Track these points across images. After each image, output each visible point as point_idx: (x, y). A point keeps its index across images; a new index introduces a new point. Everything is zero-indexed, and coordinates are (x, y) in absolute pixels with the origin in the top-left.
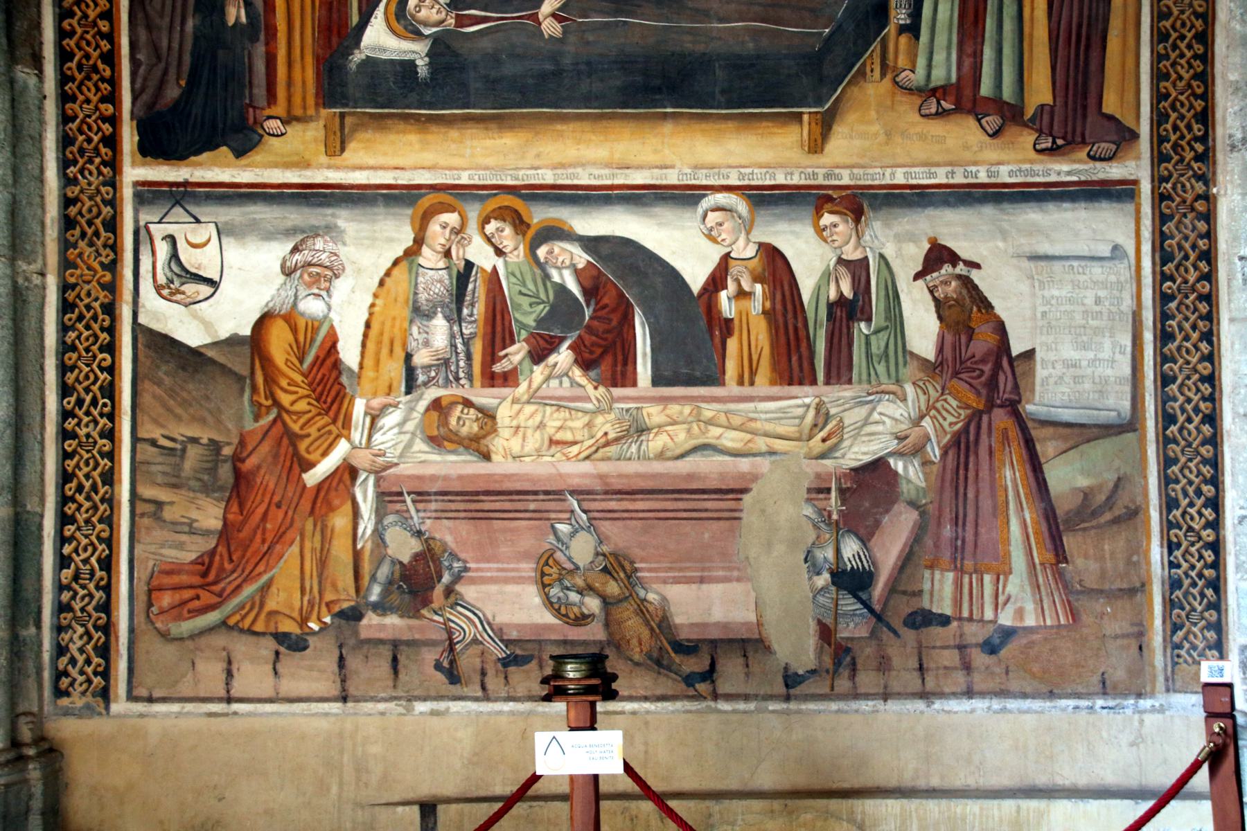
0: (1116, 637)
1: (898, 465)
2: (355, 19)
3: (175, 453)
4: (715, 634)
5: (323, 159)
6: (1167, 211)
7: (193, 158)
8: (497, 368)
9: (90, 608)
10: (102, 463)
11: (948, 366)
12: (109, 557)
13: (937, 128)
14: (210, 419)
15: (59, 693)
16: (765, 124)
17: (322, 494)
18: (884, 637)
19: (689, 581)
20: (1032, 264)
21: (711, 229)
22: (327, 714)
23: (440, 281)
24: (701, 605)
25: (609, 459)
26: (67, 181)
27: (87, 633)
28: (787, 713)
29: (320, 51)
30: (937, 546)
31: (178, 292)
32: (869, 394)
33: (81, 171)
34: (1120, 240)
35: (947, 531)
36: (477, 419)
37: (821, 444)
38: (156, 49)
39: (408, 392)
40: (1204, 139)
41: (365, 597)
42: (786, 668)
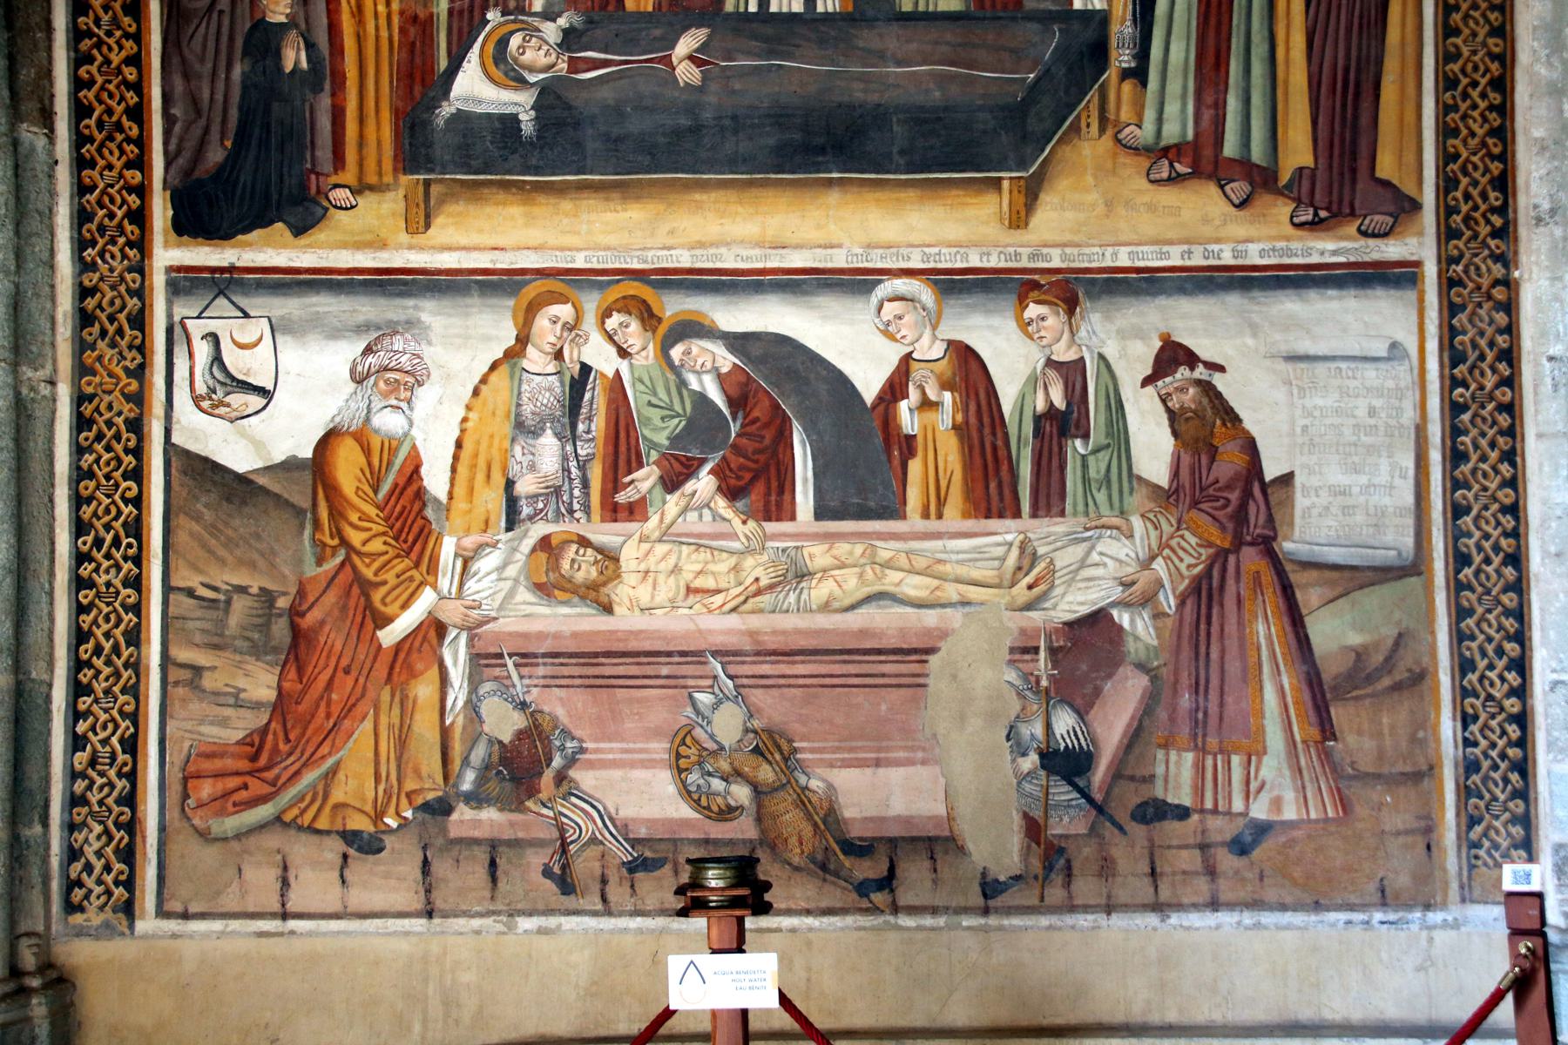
0: (1398, 833)
1: (1123, 618)
2: (443, 63)
3: (218, 606)
4: (894, 831)
5: (404, 237)
6: (1458, 300)
7: (239, 237)
8: (621, 498)
9: (110, 801)
10: (126, 618)
11: (1185, 494)
12: (135, 736)
13: (1169, 196)
14: (261, 563)
15: (71, 908)
16: (954, 192)
17: (402, 656)
18: (1107, 834)
19: (861, 764)
20: (1290, 367)
21: (888, 324)
22: (407, 934)
23: (550, 389)
24: (874, 794)
25: (761, 611)
26: (84, 266)
27: (106, 832)
28: (985, 929)
29: (400, 104)
30: (1172, 719)
31: (221, 403)
32: (1087, 529)
33: (102, 254)
34: (1400, 336)
35: (1186, 700)
36: (596, 562)
37: (1027, 592)
38: (194, 101)
39: (509, 529)
40: (1502, 210)
41: (456, 786)
42: (984, 874)
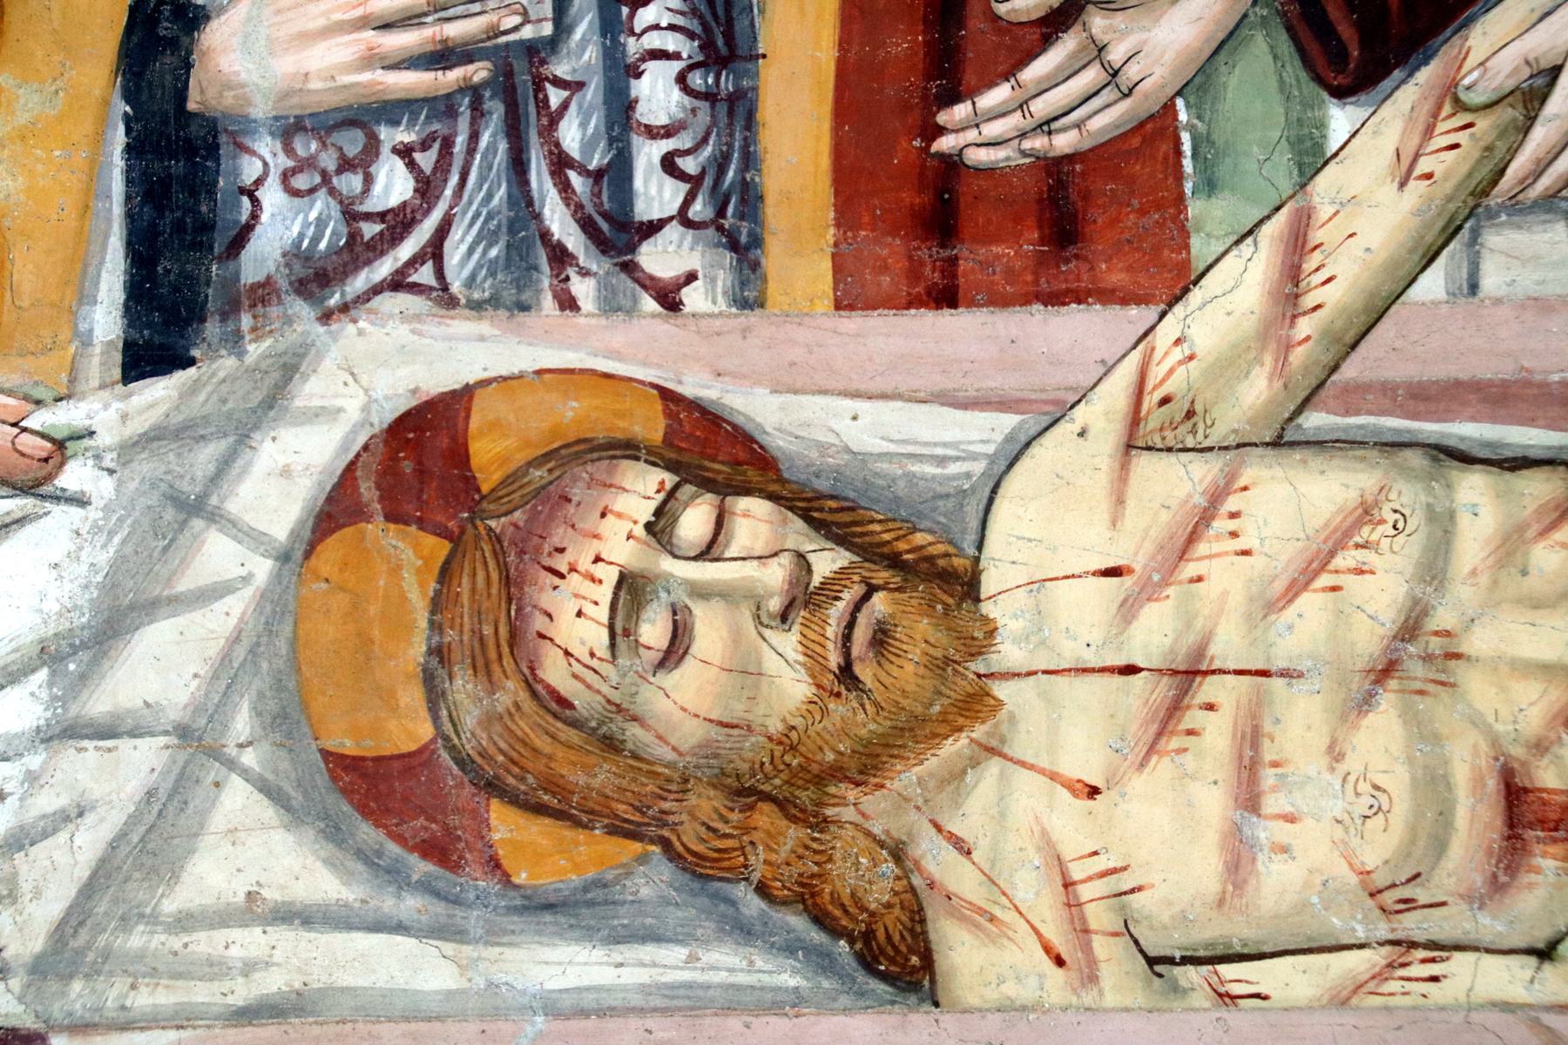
8: (988, 129)
36: (804, 599)
39: (148, 355)
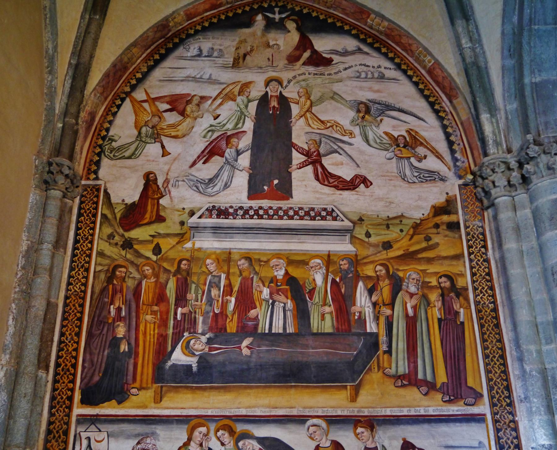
2: (169, 349)
5: (153, 405)
13: (402, 391)
16: (332, 390)
21: (311, 434)
26: (51, 414)
33: (57, 411)
40: (509, 397)
